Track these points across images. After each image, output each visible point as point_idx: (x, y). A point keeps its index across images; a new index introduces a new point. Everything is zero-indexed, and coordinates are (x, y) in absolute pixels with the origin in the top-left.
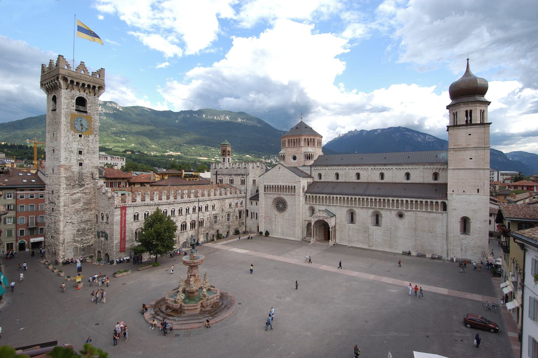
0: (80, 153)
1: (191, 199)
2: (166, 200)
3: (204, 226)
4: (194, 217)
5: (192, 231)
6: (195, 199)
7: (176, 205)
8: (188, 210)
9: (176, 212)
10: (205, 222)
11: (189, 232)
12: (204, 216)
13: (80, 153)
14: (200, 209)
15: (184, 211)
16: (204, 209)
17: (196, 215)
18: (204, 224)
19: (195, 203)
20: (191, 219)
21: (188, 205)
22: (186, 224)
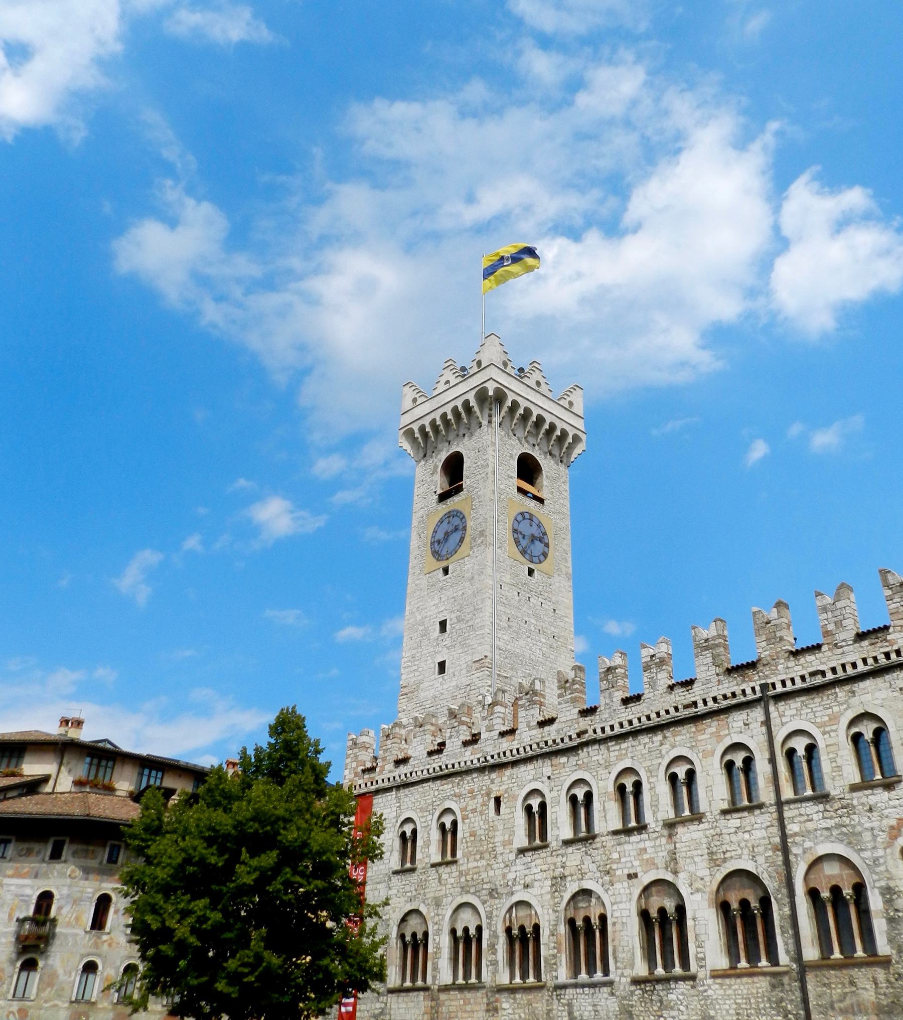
0: (443, 625)
1: (697, 693)
2: (537, 733)
3: (883, 947)
4: (749, 844)
5: (742, 986)
6: (730, 686)
7: (594, 754)
8: (684, 783)
9: (596, 805)
10: (875, 902)
11: (714, 989)
12: (852, 838)
13: (443, 625)
14: (805, 760)
15: (658, 801)
16: (840, 767)
17: (759, 828)
18: (879, 926)
19: (738, 718)
20: (714, 861)
21: (679, 742)
22: (681, 910)
